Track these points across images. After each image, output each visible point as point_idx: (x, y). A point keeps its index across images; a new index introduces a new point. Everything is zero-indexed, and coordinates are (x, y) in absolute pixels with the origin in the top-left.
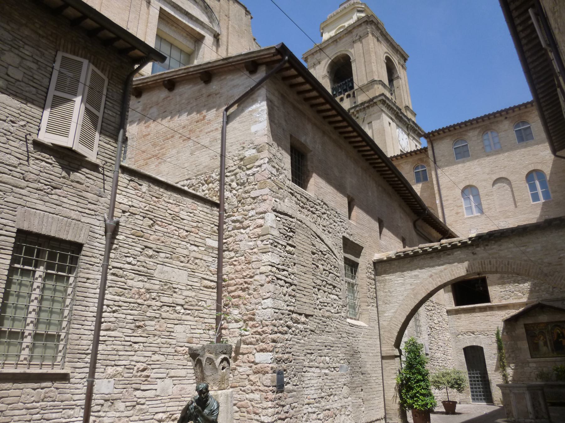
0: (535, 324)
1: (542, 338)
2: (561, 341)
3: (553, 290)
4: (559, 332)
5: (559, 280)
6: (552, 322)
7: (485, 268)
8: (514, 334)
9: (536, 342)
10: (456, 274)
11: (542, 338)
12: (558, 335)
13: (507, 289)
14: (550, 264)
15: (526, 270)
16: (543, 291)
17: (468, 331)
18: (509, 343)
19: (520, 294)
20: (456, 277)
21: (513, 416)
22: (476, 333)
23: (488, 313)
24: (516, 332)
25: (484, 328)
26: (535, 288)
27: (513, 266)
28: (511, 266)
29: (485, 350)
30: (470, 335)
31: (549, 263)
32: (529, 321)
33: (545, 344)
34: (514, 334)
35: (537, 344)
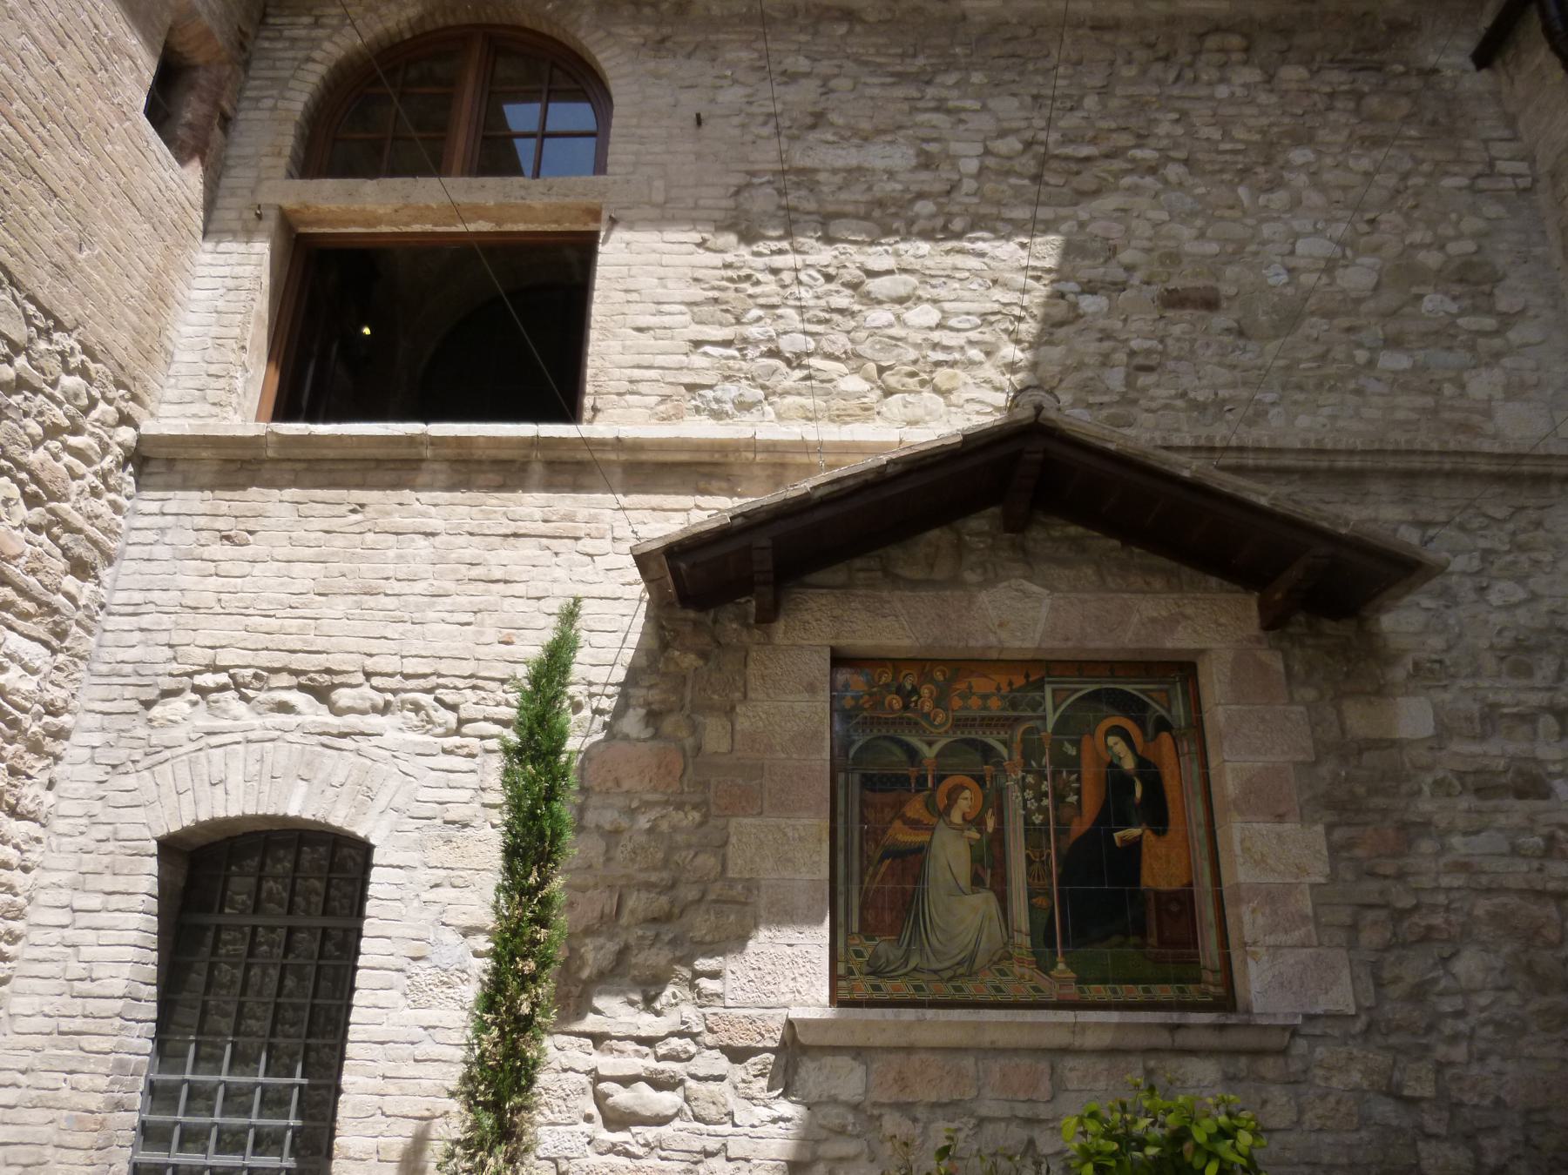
0: (922, 664)
1: (966, 803)
2: (1135, 846)
3: (1129, 382)
4: (1129, 764)
6: (1082, 667)
8: (715, 736)
9: (906, 837)
11: (966, 803)
12: (1117, 783)
13: (753, 331)
17: (279, 660)
18: (643, 822)
19: (854, 384)
22: (342, 697)
23: (531, 505)
24: (743, 724)
29: (380, 882)
30: (284, 708)
34: (715, 736)
35: (912, 861)
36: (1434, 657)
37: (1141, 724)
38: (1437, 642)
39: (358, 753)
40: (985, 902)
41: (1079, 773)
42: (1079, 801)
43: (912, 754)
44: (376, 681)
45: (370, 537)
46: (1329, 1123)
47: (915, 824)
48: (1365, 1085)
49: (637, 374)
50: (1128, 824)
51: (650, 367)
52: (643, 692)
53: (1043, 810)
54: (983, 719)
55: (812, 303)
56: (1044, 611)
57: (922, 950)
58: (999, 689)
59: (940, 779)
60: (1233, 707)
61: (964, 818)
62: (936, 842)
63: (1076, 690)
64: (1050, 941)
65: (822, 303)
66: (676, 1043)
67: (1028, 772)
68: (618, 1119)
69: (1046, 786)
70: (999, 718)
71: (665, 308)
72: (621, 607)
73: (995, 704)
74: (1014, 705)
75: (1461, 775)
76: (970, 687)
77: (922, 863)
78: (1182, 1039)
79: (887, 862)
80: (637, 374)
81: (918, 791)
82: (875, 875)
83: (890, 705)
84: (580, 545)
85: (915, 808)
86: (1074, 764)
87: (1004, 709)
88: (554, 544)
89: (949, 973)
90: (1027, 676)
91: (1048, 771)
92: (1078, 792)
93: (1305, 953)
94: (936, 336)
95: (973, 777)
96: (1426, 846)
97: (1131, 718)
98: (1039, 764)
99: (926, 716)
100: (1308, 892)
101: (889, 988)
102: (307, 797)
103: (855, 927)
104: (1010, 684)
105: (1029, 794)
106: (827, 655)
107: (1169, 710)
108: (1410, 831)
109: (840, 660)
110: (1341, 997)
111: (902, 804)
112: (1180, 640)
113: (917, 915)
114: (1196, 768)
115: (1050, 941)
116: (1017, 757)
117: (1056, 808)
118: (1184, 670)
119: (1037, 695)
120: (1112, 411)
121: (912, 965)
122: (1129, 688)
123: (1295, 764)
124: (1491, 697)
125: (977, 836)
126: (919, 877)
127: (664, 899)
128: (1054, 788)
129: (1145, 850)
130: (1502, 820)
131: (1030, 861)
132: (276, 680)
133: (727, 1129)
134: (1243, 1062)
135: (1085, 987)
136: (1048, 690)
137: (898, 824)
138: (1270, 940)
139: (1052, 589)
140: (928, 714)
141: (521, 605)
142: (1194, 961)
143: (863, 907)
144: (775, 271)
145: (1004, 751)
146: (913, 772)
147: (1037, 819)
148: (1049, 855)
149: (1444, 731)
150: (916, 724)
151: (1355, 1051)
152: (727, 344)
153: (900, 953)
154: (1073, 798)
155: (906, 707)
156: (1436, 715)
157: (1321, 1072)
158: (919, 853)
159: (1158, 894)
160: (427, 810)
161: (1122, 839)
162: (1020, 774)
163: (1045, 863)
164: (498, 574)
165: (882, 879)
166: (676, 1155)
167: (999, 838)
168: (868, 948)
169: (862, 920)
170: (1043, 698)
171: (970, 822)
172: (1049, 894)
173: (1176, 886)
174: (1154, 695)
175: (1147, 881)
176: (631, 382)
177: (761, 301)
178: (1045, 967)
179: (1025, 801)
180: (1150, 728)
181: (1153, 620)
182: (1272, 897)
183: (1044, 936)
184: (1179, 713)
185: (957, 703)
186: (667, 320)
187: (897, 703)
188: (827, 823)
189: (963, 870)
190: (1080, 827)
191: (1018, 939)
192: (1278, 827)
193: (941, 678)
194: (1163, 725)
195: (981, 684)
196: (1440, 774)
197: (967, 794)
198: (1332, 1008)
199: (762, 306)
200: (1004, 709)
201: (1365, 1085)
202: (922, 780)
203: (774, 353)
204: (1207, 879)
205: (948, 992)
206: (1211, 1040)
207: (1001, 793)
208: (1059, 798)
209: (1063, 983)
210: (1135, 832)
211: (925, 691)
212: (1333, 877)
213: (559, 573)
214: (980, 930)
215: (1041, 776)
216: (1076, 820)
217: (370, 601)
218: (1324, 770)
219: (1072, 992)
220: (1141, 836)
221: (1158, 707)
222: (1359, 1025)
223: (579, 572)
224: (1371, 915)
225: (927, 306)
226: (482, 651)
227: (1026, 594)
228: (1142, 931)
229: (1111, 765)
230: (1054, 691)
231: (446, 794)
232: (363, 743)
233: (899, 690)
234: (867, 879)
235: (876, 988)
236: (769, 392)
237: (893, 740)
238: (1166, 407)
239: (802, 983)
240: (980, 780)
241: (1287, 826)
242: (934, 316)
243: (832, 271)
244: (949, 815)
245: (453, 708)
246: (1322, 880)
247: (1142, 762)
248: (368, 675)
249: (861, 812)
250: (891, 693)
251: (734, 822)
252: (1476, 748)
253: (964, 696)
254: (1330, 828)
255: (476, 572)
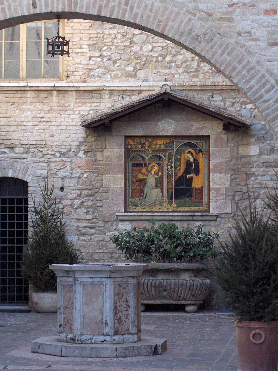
0: (146, 137)
1: (155, 169)
2: (192, 178)
5: (219, 51)
7: (76, 5)
9: (141, 177)
10: (10, 8)
11: (155, 169)
14: (209, 14)
15: (160, 22)
16: (178, 67)
18: (85, 176)
20: (8, 17)
21: (71, 330)
22: (17, 150)
24: (106, 154)
25: (37, 138)
26: (164, 57)
27: (135, 10)
28: (132, 9)
31: (206, 13)
32: (138, 131)
33: (159, 183)
34: (99, 156)
35: (143, 182)
36: (262, 136)
37: (195, 151)
38: (263, 132)
39: (22, 162)
40: (158, 190)
41: (180, 162)
42: (180, 169)
43: (143, 158)
44: (24, 146)
45: (17, 111)
46: (223, 234)
47: (143, 174)
48: (231, 226)
49: (77, 66)
50: (190, 173)
51: (80, 64)
52: (83, 147)
53: (172, 171)
54: (159, 150)
55: (120, 44)
56: (173, 127)
57: (145, 201)
58: (163, 143)
59: (149, 164)
60: (214, 148)
61: (154, 173)
62: (148, 177)
63: (181, 143)
64: (172, 198)
65: (122, 44)
66: (94, 220)
67: (169, 162)
68: (84, 234)
69: (173, 165)
70: (163, 150)
71: (83, 46)
72: (77, 128)
73: (162, 146)
74: (167, 147)
75: (263, 163)
76: (157, 143)
77: (145, 183)
78: (194, 218)
79: (137, 182)
80: (77, 66)
81: (144, 167)
82: (135, 185)
83: (139, 147)
84: (66, 113)
85: (144, 171)
86: (179, 160)
87: (164, 148)
88: (62, 113)
89: (150, 205)
90: (170, 140)
91: (173, 162)
92: (180, 166)
93: (222, 201)
94: (150, 54)
95: (157, 164)
96: (252, 178)
97: (193, 149)
98: (172, 161)
99: (147, 150)
100: (225, 189)
101: (138, 209)
102: (13, 173)
103: (130, 196)
104: (166, 142)
105: (169, 167)
106: (124, 138)
107: (202, 148)
108: (248, 175)
109: (126, 137)
110: (229, 210)
111: (141, 170)
112: (204, 133)
113: (143, 194)
114: (207, 160)
115: (172, 198)
116: (167, 159)
117: (175, 170)
118: (207, 137)
119: (172, 144)
120: (194, 73)
121: (142, 204)
122: (193, 142)
123: (226, 161)
124: (273, 145)
125: (157, 177)
126: (144, 186)
127: (90, 192)
128: (175, 166)
129: (194, 179)
130: (270, 173)
131: (168, 182)
132: (3, 146)
133: (105, 236)
134: (207, 222)
135: (179, 208)
136: (175, 143)
137: (140, 174)
138: (216, 199)
139: (175, 120)
140: (147, 149)
141: (54, 128)
142: (202, 202)
143: (132, 192)
144: (110, 34)
145: (164, 158)
146: (143, 163)
147: (170, 173)
148: (172, 180)
149: (261, 153)
150: (144, 151)
151: (230, 220)
152: (99, 57)
153: (140, 201)
154: (179, 168)
155: (142, 148)
156: (260, 149)
157: (222, 224)
158: (145, 180)
159: (196, 188)
160: (39, 175)
161: (189, 177)
162: (167, 163)
163: (172, 182)
164: (48, 120)
165: (136, 187)
166: (95, 241)
167: (162, 177)
168: (133, 200)
169: (132, 195)
170: (174, 145)
171: (156, 173)
172: (172, 189)
173: (200, 187)
174: (199, 144)
175: (194, 185)
176: (75, 68)
177: (107, 44)
178: (170, 204)
179: (168, 169)
180: (197, 152)
181: (198, 128)
182: (217, 190)
183: (170, 198)
184: (204, 148)
185: (154, 146)
186: (84, 50)
187: (140, 146)
188: (123, 176)
189: (154, 185)
190: (180, 174)
191: (165, 198)
192: (220, 175)
193: (150, 141)
194: (200, 151)
195: (159, 142)
196: (258, 163)
197: (155, 167)
198: (227, 212)
199: (107, 45)
200: (164, 148)
201: (231, 226)
202: (145, 164)
203: (109, 59)
204: (206, 185)
205: (148, 209)
206: (200, 218)
207: (163, 167)
208: (175, 168)
209: (174, 207)
210: (192, 175)
211: (147, 144)
212: (231, 185)
213: (62, 120)
214: (157, 197)
215: (172, 163)
216: (179, 173)
217: (20, 127)
218: (232, 163)
219: (176, 209)
220: (193, 176)
221: (200, 147)
222: (232, 215)
223: (67, 120)
224: (238, 193)
225: (149, 44)
226: (46, 139)
227: (169, 122)
228: (191, 196)
229: (188, 160)
230: (176, 143)
231: (42, 171)
232: (24, 161)
233: (141, 144)
234: (133, 186)
235: (135, 209)
236: (110, 70)
237: (139, 155)
238: (207, 72)
239: (119, 209)
240: (158, 164)
241: (222, 175)
242: (150, 48)
243: (125, 34)
244: (151, 172)
245: (42, 151)
246: (228, 186)
247: (195, 160)
248: (22, 144)
249: (132, 172)
250: (138, 144)
251: (104, 176)
252: (267, 157)
253: (155, 145)
254: (231, 175)
255: (43, 120)
